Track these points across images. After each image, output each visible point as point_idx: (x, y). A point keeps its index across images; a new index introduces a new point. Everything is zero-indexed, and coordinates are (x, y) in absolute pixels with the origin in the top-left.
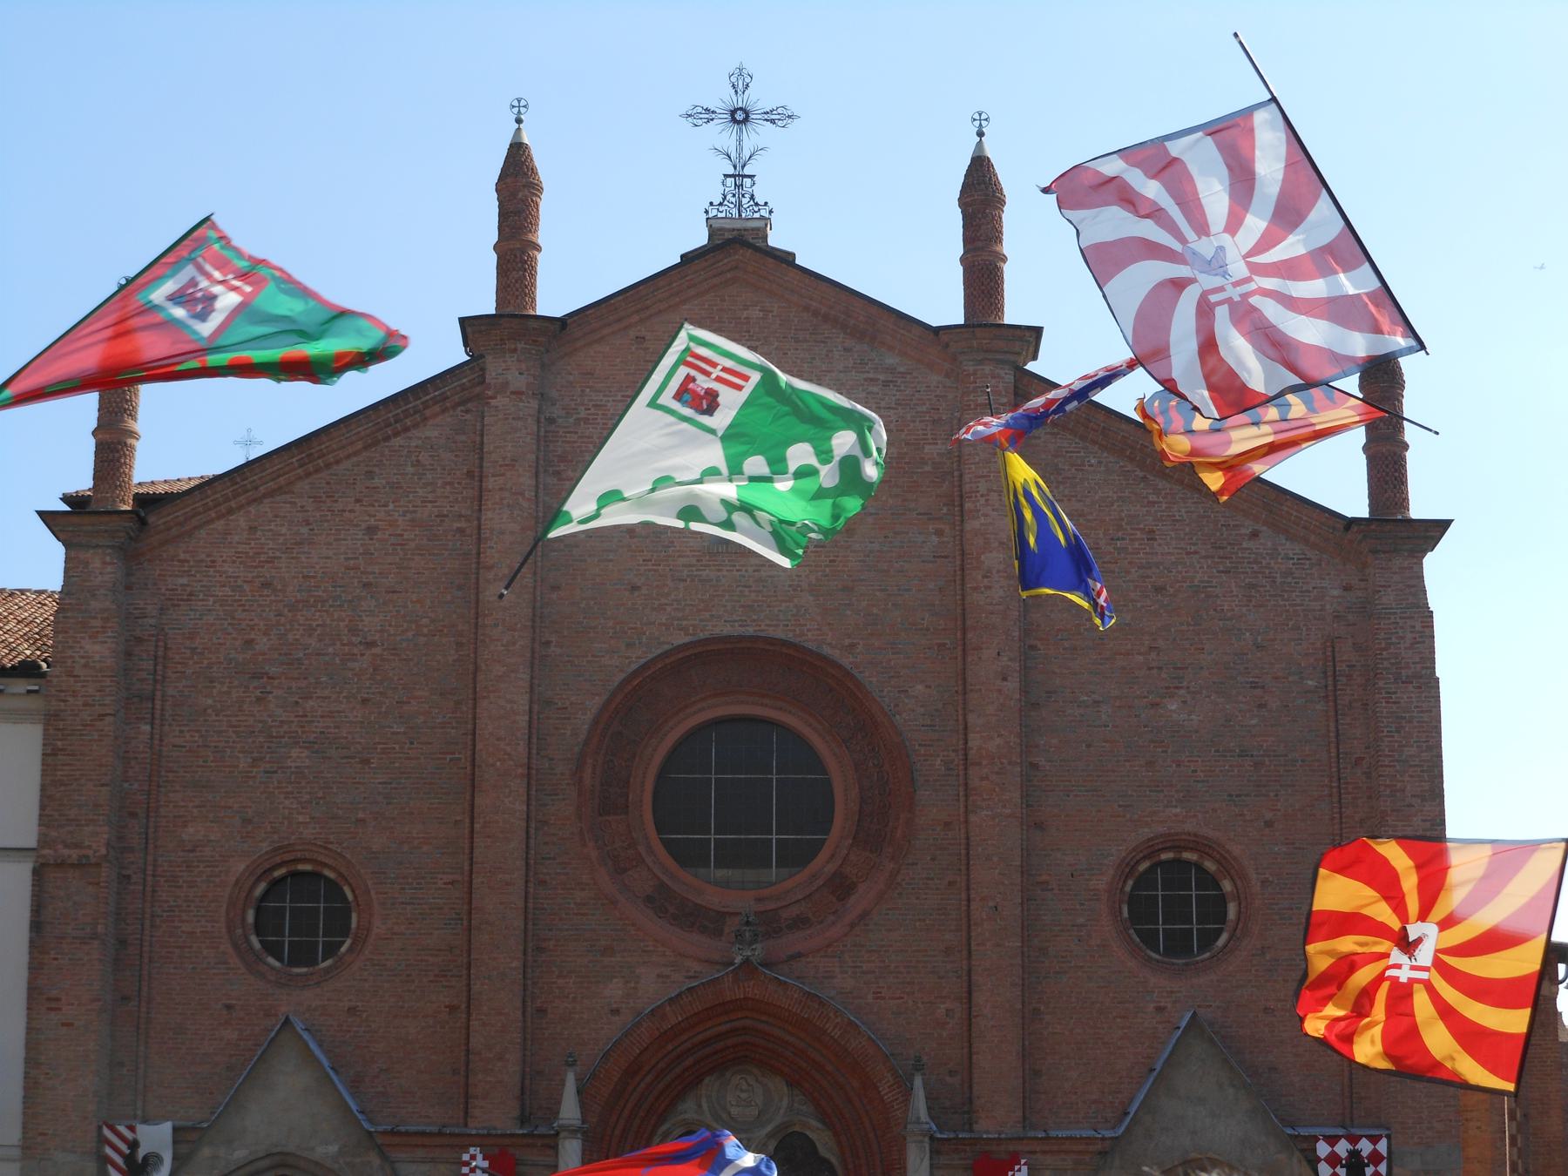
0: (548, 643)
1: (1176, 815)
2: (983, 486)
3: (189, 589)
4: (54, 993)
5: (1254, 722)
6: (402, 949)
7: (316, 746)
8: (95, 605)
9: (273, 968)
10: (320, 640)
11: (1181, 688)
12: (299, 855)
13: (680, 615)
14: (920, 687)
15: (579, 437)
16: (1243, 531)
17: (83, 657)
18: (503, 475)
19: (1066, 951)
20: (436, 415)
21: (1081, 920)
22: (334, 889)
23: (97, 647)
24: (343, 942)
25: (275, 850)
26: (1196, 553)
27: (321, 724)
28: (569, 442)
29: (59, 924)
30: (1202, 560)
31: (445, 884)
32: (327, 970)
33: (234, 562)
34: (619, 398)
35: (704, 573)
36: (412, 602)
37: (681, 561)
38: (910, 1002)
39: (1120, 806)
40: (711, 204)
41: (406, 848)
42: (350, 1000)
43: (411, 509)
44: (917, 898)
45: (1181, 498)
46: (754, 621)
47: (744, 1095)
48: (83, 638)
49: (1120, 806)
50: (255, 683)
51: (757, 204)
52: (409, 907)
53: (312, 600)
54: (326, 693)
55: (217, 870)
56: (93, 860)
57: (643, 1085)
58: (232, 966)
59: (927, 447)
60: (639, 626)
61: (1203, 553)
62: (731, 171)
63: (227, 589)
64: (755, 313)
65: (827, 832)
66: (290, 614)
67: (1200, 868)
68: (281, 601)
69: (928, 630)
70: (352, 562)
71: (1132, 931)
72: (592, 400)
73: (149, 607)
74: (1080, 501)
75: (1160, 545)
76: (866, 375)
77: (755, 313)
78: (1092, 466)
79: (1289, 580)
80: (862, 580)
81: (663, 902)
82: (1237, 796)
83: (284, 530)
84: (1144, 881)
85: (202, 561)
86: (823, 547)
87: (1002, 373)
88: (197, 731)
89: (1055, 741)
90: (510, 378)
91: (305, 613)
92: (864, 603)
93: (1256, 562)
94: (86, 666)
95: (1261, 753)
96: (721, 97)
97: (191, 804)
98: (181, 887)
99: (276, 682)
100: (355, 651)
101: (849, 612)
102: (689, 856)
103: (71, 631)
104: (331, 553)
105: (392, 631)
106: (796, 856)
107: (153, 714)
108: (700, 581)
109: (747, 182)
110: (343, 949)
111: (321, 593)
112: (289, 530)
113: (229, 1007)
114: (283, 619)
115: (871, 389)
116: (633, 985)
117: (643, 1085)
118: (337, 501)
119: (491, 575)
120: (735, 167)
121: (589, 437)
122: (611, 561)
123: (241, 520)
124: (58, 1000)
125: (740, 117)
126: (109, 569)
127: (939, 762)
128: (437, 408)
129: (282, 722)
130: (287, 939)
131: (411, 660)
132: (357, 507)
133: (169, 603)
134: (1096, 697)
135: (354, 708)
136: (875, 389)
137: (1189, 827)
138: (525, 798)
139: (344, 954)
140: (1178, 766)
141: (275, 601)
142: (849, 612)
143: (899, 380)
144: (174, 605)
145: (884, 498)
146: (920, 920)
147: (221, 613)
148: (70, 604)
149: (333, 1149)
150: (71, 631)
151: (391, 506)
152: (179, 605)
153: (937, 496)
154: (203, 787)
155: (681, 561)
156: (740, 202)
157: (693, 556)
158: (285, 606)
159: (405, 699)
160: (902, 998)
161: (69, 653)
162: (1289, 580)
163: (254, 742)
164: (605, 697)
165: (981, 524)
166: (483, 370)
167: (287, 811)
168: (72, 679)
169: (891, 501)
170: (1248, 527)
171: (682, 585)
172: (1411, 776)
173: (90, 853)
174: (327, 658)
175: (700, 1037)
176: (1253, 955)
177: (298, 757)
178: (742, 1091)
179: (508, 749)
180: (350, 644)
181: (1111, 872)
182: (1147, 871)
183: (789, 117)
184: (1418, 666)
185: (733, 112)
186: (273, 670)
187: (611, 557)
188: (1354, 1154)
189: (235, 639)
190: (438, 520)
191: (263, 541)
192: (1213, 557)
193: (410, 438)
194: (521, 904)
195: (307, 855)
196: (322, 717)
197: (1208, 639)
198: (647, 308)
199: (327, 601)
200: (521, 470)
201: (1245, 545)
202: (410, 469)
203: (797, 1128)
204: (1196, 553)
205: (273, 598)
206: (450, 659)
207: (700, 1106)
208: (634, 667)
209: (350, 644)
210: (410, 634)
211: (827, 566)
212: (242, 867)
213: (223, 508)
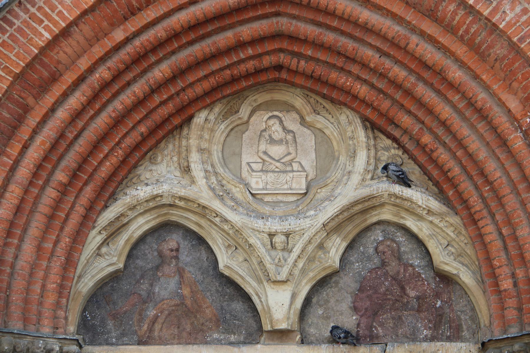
47: (277, 151)
57: (62, 114)
117: (62, 114)
178: (272, 141)
203: (386, 215)
207: (187, 170)
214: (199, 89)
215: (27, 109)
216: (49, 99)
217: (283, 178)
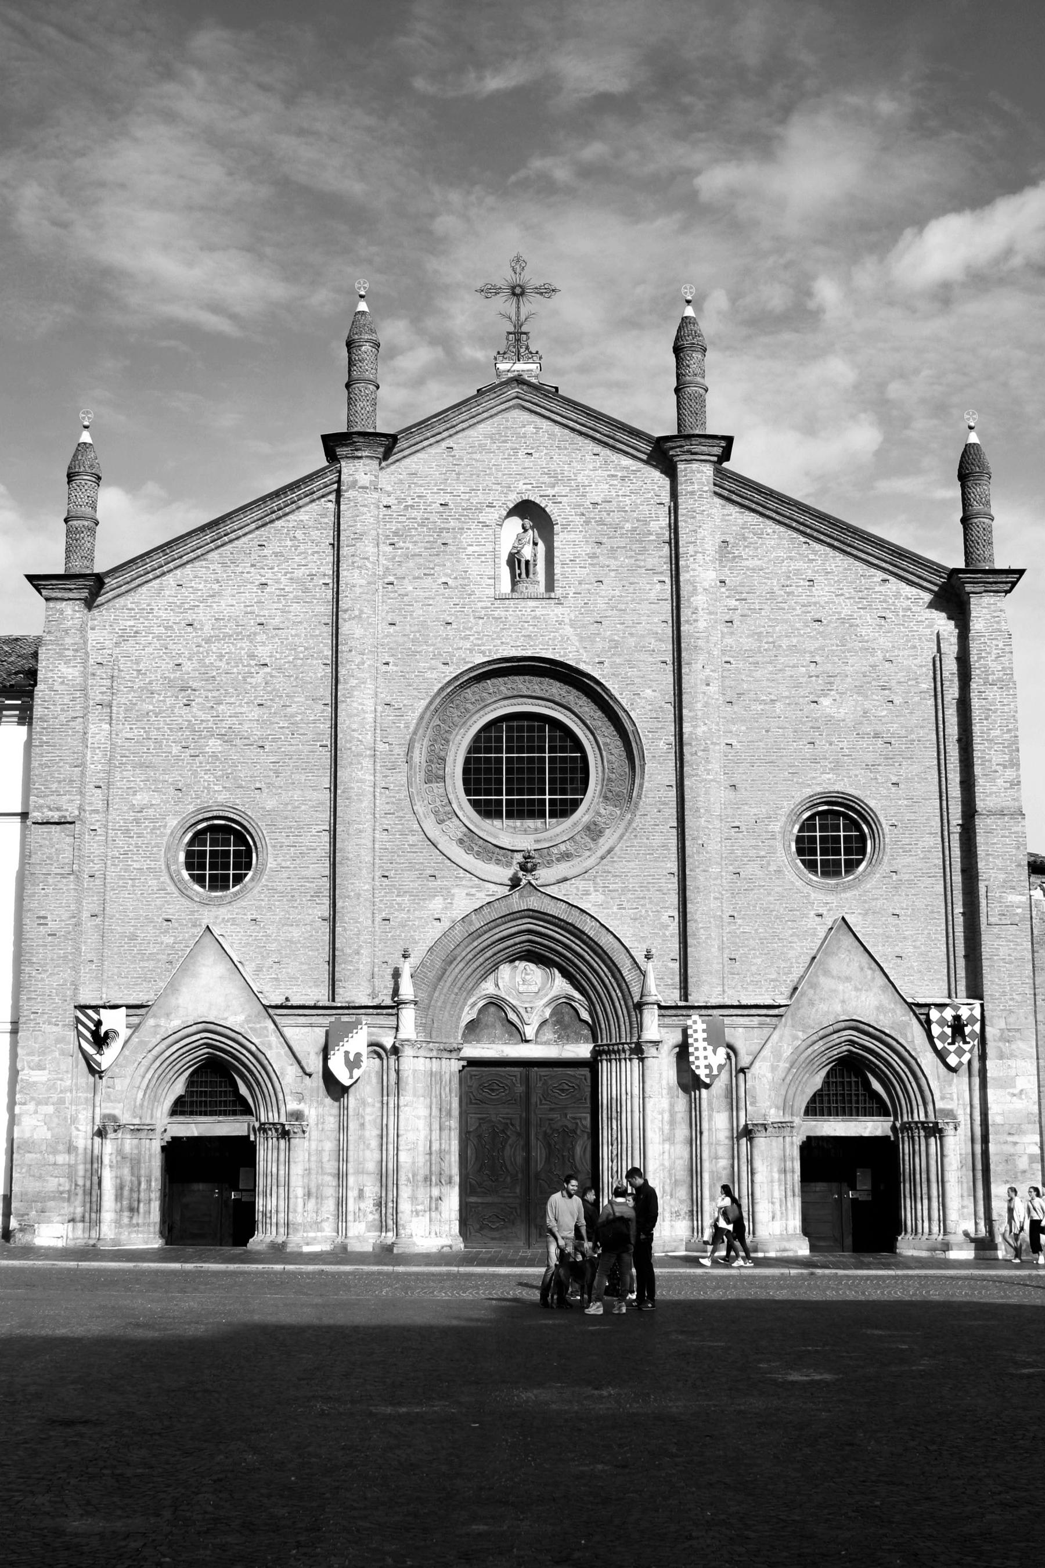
0: (387, 664)
1: (829, 779)
2: (691, 549)
3: (135, 629)
4: (42, 913)
5: (884, 713)
6: (288, 878)
7: (226, 737)
8: (68, 640)
9: (198, 893)
10: (228, 664)
11: (832, 690)
12: (215, 814)
13: (480, 642)
14: (649, 691)
15: (407, 519)
16: (875, 579)
17: (60, 677)
18: (354, 545)
19: (752, 875)
20: (307, 504)
21: (763, 853)
22: (241, 839)
23: (70, 670)
24: (246, 875)
25: (198, 810)
26: (842, 595)
27: (229, 722)
28: (400, 522)
29: (46, 864)
30: (847, 600)
31: (318, 832)
32: (235, 894)
33: (166, 609)
34: (436, 491)
35: (496, 613)
36: (292, 636)
37: (480, 605)
38: (643, 911)
39: (789, 773)
40: (499, 353)
41: (290, 807)
42: (252, 914)
43: (290, 570)
44: (648, 839)
45: (832, 557)
46: (531, 646)
48: (59, 664)
49: (789, 773)
50: (183, 694)
51: (531, 353)
52: (292, 849)
53: (221, 635)
54: (233, 700)
55: (157, 825)
56: (69, 820)
58: (169, 891)
59: (652, 523)
60: (450, 650)
61: (847, 595)
62: (512, 329)
63: (162, 628)
64: (530, 429)
65: (584, 792)
66: (206, 645)
67: (846, 817)
68: (200, 636)
69: (654, 651)
70: (249, 608)
71: (798, 861)
72: (415, 493)
73: (107, 642)
74: (760, 559)
75: (817, 590)
76: (609, 473)
77: (530, 429)
78: (768, 535)
79: (909, 613)
80: (606, 617)
81: (470, 840)
82: (872, 765)
83: (201, 587)
84: (807, 825)
85: (144, 609)
86: (580, 593)
87: (705, 469)
88: (144, 728)
89: (743, 728)
90: (357, 477)
91: (216, 644)
92: (609, 633)
93: (885, 601)
94: (62, 683)
95: (889, 735)
96: (504, 276)
97: (138, 779)
98: (133, 837)
99: (197, 693)
100: (253, 670)
101: (598, 639)
102: (488, 810)
103: (51, 659)
104: (234, 602)
105: (278, 656)
106: (564, 810)
107: (111, 717)
108: (493, 618)
109: (524, 337)
110: (247, 878)
111: (227, 631)
112: (205, 586)
113: (168, 920)
114: (201, 649)
115: (612, 482)
116: (449, 901)
118: (238, 566)
119: (346, 616)
120: (515, 326)
121: (414, 519)
122: (430, 605)
123: (170, 580)
124: (46, 918)
125: (518, 292)
126: (78, 615)
127: (662, 743)
128: (307, 499)
129: (201, 720)
130: (207, 872)
131: (292, 676)
132: (252, 570)
133: (121, 639)
134: (773, 697)
135: (252, 710)
136: (615, 482)
137: (837, 788)
138: (372, 772)
139: (247, 883)
140: (831, 744)
141: (196, 637)
142: (598, 639)
143: (632, 476)
144: (124, 640)
145: (622, 559)
146: (649, 854)
147: (158, 645)
148: (51, 640)
149: (241, 1018)
150: (51, 659)
151: (276, 569)
152: (128, 640)
153: (660, 557)
154: (147, 767)
155: (480, 605)
156: (519, 351)
157: (489, 601)
158: (202, 640)
159: (288, 704)
160: (638, 908)
161: (50, 674)
162: (909, 613)
163: (182, 735)
164: (428, 701)
165: (691, 576)
166: (340, 472)
167: (206, 784)
168: (53, 693)
169: (626, 560)
170: (880, 575)
171: (481, 621)
172: (996, 751)
173: (67, 814)
174: (233, 676)
175: (497, 937)
176: (884, 877)
177: (214, 745)
179: (360, 737)
180: (249, 665)
181: (784, 819)
182: (809, 819)
183: (553, 290)
184: (1001, 673)
185: (513, 288)
186: (195, 685)
187: (431, 603)
188: (957, 1018)
189: (167, 663)
190: (309, 578)
191: (186, 594)
192: (853, 598)
193: (289, 521)
194: (370, 845)
195: (221, 814)
196: (230, 717)
197: (851, 656)
198: (454, 427)
199: (232, 636)
200: (366, 541)
201: (877, 589)
202: (289, 543)
204: (842, 595)
205: (194, 634)
206: (319, 675)
208: (448, 679)
209: (249, 665)
210: (291, 658)
211: (582, 607)
212: (176, 822)
213: (158, 572)
214: (501, 958)
215: (446, 970)
216: (453, 966)
217: (530, 987)
